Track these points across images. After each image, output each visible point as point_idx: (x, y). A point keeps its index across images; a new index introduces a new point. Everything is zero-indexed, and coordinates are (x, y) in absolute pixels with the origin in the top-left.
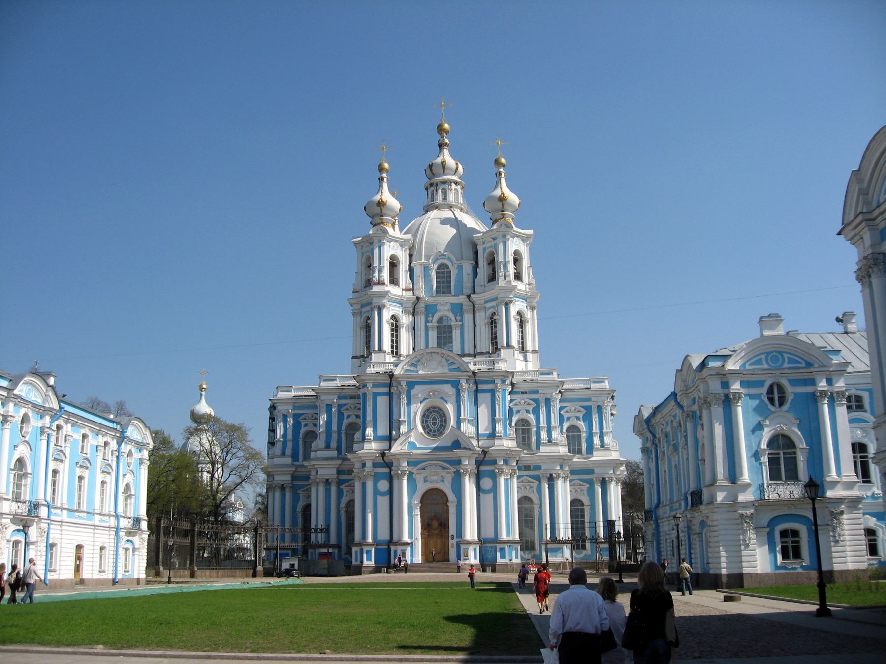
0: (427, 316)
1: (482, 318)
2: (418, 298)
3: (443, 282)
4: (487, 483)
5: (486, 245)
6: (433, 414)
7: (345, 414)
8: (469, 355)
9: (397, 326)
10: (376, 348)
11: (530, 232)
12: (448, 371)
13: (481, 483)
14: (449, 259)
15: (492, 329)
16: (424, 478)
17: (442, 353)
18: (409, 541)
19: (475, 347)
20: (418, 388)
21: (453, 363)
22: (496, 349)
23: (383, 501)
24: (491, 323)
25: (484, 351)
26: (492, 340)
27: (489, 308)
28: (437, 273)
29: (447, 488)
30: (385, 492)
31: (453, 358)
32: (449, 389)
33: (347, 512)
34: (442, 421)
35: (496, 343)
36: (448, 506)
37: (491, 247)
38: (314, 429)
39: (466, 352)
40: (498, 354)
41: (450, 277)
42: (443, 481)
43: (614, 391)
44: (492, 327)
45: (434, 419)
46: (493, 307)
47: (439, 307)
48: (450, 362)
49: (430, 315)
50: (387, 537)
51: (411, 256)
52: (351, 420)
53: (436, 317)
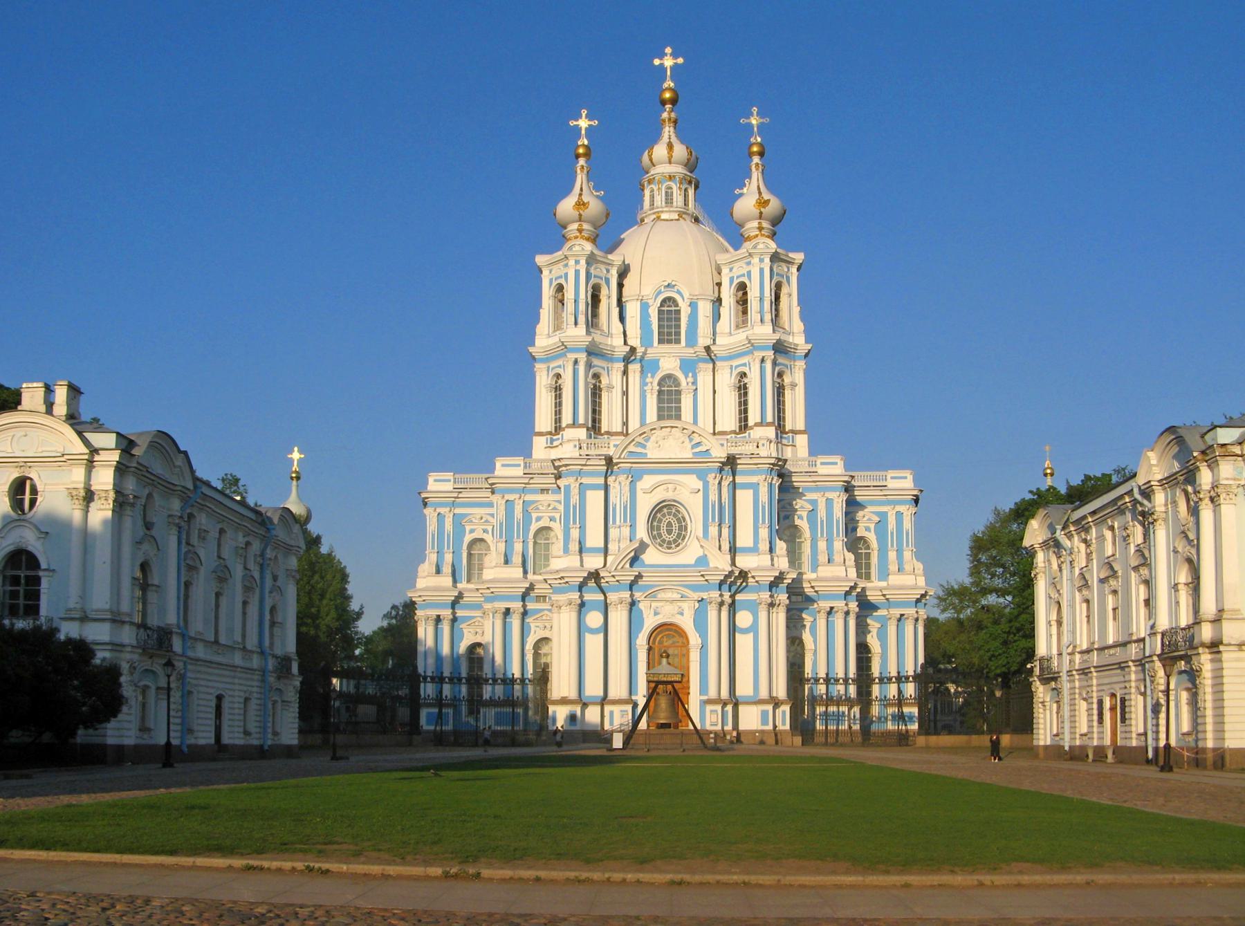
1: (726, 380)
2: (633, 350)
3: (669, 327)
4: (744, 619)
5: (736, 272)
6: (668, 517)
7: (534, 516)
10: (571, 422)
11: (799, 257)
12: (691, 456)
13: (737, 618)
14: (679, 292)
15: (740, 398)
16: (655, 610)
17: (684, 429)
18: (633, 698)
19: (714, 424)
20: (647, 482)
21: (699, 444)
23: (594, 643)
24: (739, 388)
26: (740, 413)
27: (736, 367)
28: (660, 312)
29: (686, 622)
30: (597, 629)
31: (700, 435)
32: (693, 482)
33: (536, 655)
34: (680, 528)
35: (746, 419)
36: (688, 651)
37: (744, 275)
38: (488, 537)
40: (749, 434)
41: (679, 319)
42: (682, 614)
43: (921, 491)
44: (740, 395)
45: (669, 524)
46: (744, 365)
48: (694, 443)
49: (649, 375)
50: (601, 694)
51: (620, 286)
52: (541, 524)
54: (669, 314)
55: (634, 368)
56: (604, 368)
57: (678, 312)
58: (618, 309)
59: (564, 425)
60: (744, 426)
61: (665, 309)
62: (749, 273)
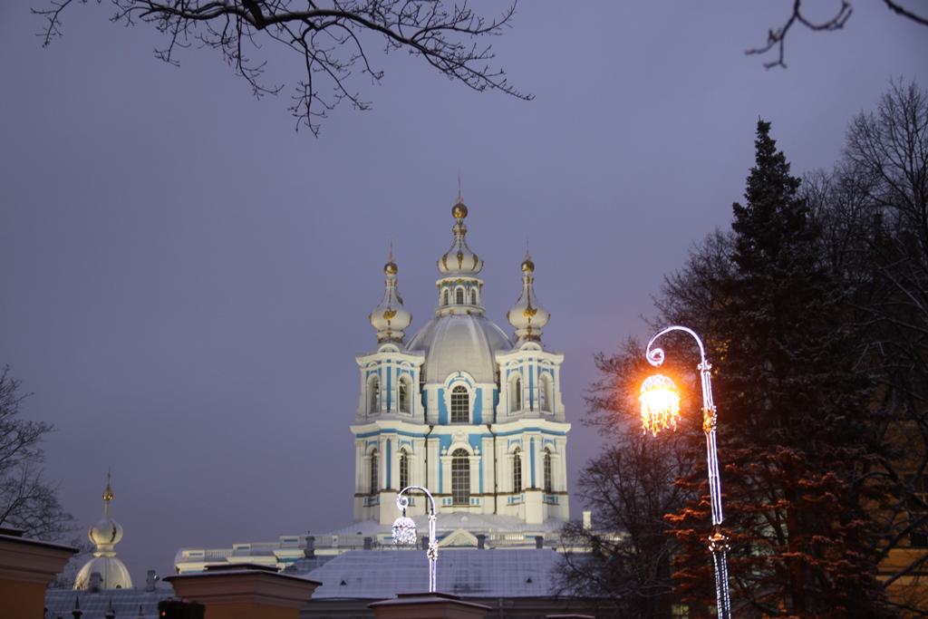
0: (441, 449)
1: (504, 448)
5: (510, 367)
8: (489, 494)
9: (406, 460)
10: (384, 487)
14: (467, 381)
19: (496, 486)
22: (518, 489)
25: (505, 490)
27: (513, 442)
28: (453, 397)
39: (486, 491)
41: (467, 402)
46: (518, 441)
47: (455, 438)
51: (422, 374)
53: (452, 448)
54: (460, 399)
55: (434, 445)
56: (409, 443)
57: (467, 396)
58: (420, 395)
59: (378, 490)
60: (518, 489)
61: (457, 394)
62: (522, 368)
